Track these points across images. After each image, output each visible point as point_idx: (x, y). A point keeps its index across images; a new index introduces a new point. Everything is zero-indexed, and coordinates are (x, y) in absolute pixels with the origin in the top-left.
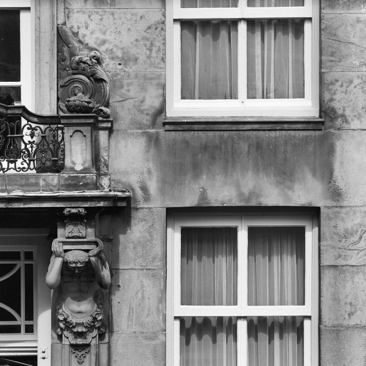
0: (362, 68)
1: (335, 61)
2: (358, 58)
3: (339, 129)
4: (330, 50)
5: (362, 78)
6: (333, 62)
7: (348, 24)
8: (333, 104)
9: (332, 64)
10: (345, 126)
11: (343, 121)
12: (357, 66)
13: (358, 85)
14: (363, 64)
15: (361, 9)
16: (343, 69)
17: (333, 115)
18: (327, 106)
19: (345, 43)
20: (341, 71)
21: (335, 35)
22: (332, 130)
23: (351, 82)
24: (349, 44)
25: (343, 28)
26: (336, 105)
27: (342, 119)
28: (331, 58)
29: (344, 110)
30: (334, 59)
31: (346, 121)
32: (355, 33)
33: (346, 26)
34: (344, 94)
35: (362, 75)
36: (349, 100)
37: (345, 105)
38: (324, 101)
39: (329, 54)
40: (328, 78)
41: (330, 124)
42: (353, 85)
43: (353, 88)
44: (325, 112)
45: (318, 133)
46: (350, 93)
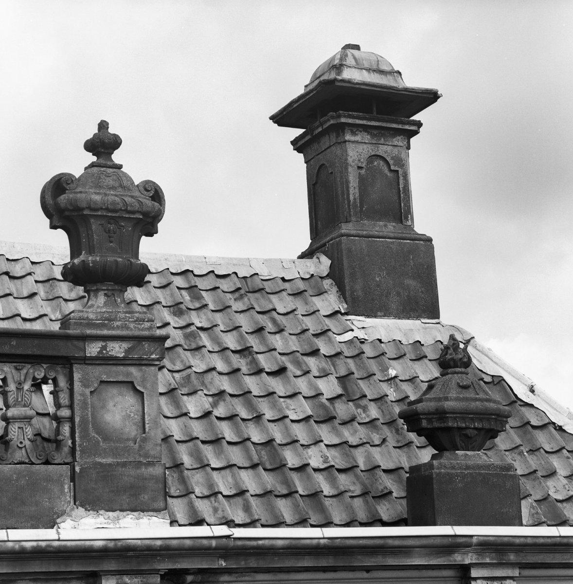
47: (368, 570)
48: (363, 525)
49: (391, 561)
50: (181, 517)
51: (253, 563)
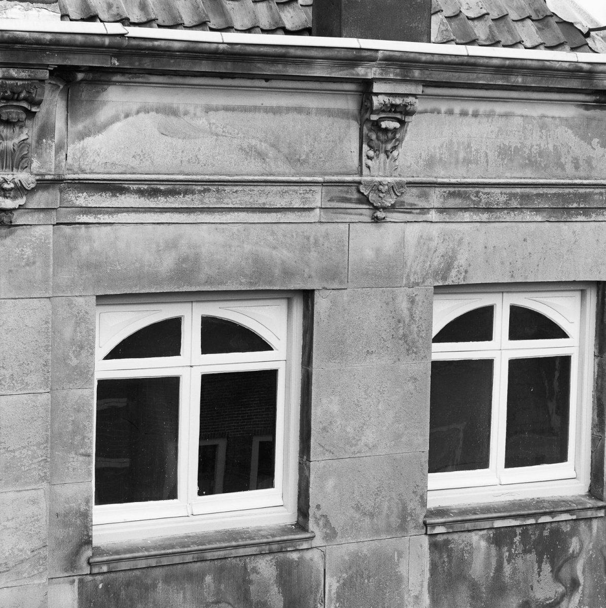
47: (267, 78)
48: (264, 31)
49: (291, 71)
50: (73, 12)
51: (147, 64)
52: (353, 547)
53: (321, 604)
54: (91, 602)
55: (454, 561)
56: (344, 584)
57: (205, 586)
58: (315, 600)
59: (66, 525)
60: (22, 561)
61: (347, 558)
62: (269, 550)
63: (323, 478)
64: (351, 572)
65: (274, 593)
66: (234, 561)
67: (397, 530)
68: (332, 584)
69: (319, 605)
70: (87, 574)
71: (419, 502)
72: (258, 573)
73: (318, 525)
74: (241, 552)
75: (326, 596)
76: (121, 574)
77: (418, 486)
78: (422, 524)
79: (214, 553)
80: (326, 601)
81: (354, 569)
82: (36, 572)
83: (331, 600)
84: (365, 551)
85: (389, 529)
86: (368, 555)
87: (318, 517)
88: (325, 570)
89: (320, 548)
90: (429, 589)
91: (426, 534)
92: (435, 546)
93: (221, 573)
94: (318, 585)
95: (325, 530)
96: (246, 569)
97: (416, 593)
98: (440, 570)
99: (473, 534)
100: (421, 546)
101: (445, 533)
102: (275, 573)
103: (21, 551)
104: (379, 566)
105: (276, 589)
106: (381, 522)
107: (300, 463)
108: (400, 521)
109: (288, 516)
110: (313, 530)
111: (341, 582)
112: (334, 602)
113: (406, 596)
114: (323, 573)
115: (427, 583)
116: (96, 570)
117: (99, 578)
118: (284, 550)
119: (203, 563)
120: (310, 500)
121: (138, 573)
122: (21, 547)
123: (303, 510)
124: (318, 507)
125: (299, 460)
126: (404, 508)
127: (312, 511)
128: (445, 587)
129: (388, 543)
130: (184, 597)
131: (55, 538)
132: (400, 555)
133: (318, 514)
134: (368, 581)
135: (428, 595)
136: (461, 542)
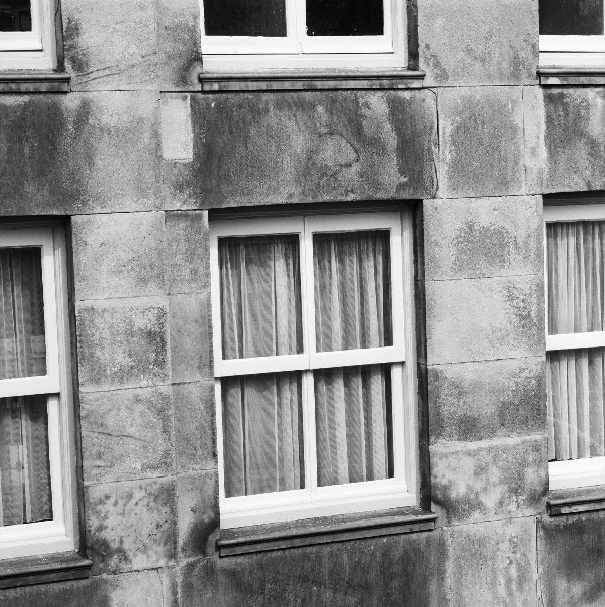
0: (145, 473)
1: (104, 467)
2: (139, 458)
3: (115, 573)
4: (96, 449)
5: (146, 490)
6: (102, 468)
7: (122, 407)
8: (104, 534)
9: (99, 471)
10: (124, 566)
11: (121, 560)
12: (138, 471)
13: (141, 500)
14: (148, 468)
15: (140, 381)
16: (117, 478)
17: (105, 552)
18: (95, 538)
19: (118, 436)
20: (115, 482)
21: (102, 425)
22: (104, 576)
23: (130, 497)
24: (125, 438)
25: (114, 412)
26: (109, 535)
27: (119, 557)
28: (98, 463)
29: (121, 542)
30: (102, 463)
31: (126, 559)
32: (133, 419)
33: (119, 409)
34: (120, 517)
35: (146, 485)
36: (128, 525)
37: (123, 534)
38: (90, 531)
39: (95, 456)
40: (94, 494)
41: (101, 566)
42: (133, 501)
43: (134, 507)
44: (92, 549)
45: (83, 582)
46: (130, 515)
52: (465, 91)
53: (435, 146)
54: (204, 120)
55: (570, 116)
56: (458, 128)
57: (317, 115)
58: (429, 141)
59: (175, 39)
60: (133, 66)
61: (459, 102)
62: (380, 85)
63: (430, 17)
64: (464, 117)
65: (387, 130)
66: (345, 93)
67: (509, 78)
68: (446, 127)
69: (433, 147)
70: (198, 92)
71: (531, 51)
72: (370, 108)
73: (428, 64)
74: (352, 84)
75: (440, 139)
76: (233, 95)
77: (529, 34)
78: (535, 74)
79: (325, 83)
80: (440, 143)
81: (467, 114)
82: (147, 78)
83: (445, 143)
84: (478, 97)
85: (501, 75)
86: (481, 101)
87: (428, 56)
88: (438, 112)
89: (431, 89)
90: (545, 141)
91: (540, 85)
92: (549, 98)
93: (331, 106)
94: (432, 127)
95: (435, 71)
96: (357, 103)
97: (533, 145)
98: (556, 123)
99: (589, 90)
100: (535, 97)
101: (559, 86)
102: (387, 110)
103: (132, 55)
104: (493, 113)
105: (389, 126)
106: (493, 70)
107: (408, 6)
108: (512, 69)
109: (397, 63)
110: (424, 69)
111: (455, 125)
112: (448, 145)
113: (522, 147)
114: (436, 114)
115: (544, 136)
116: (207, 87)
117: (211, 96)
118: (395, 87)
119: (314, 93)
120: (419, 38)
121: (249, 95)
122: (131, 51)
123: (413, 54)
124: (428, 46)
125: (407, 4)
126: (516, 57)
127: (421, 50)
128: (562, 142)
129: (503, 92)
130: (297, 125)
131: (165, 51)
132: (514, 103)
133: (428, 54)
134: (483, 127)
135: (545, 148)
136: (577, 97)
